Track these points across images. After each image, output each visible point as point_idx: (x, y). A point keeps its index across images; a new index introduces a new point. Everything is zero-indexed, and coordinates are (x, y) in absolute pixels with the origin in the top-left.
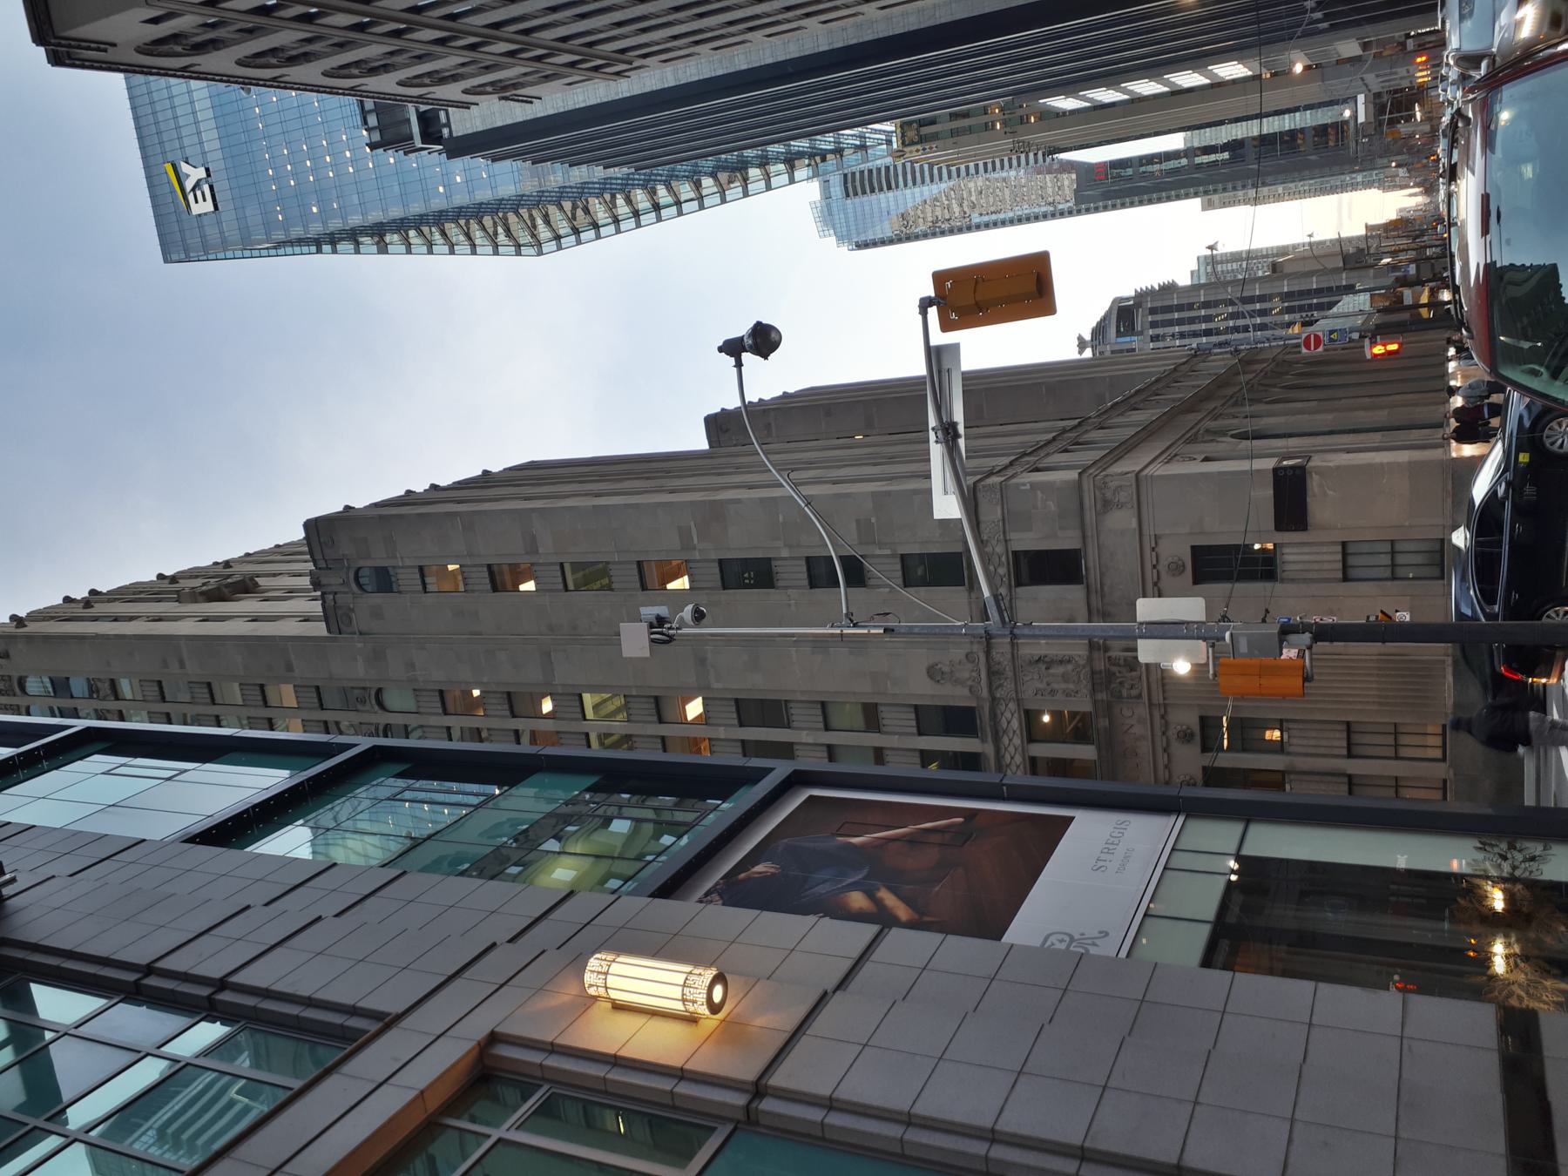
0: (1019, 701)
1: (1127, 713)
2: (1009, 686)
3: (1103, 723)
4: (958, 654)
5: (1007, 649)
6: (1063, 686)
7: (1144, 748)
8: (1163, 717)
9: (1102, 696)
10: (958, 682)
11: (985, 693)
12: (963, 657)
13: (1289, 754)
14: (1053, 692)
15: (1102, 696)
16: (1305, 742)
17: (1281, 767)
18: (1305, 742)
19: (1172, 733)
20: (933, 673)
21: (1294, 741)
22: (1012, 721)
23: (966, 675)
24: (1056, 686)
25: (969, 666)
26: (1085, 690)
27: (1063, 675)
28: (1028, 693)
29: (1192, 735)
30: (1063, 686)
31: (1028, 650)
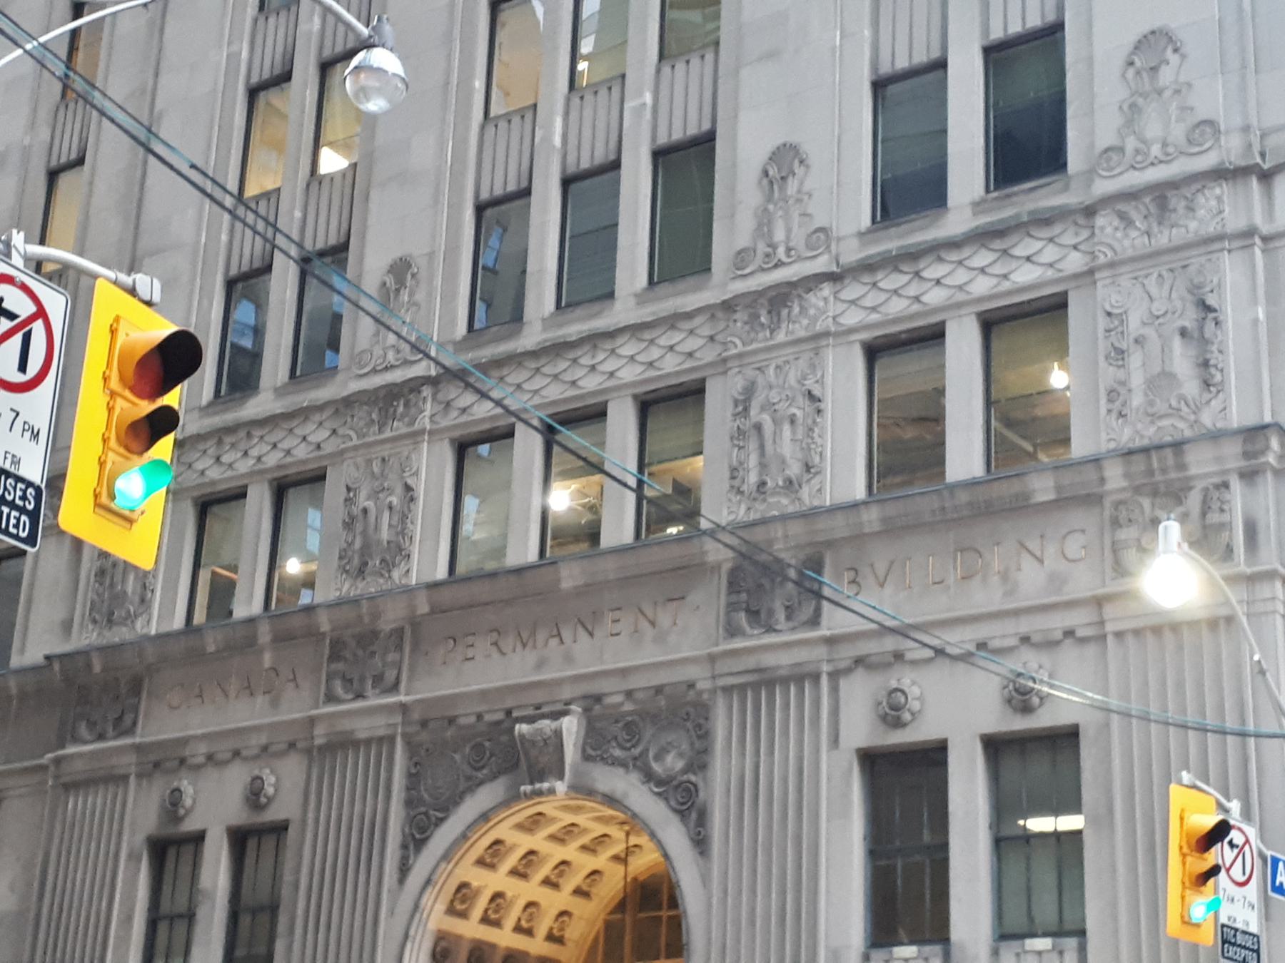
0: (1089, 274)
1: (1074, 546)
2: (1131, 242)
3: (1042, 487)
4: (1212, 99)
5: (1235, 222)
6: (1137, 380)
7: (984, 597)
8: (1069, 633)
9: (1115, 476)
10: (1132, 112)
11: (1103, 187)
12: (1202, 114)
14: (1119, 354)
15: (1115, 476)
19: (1028, 661)
20: (1154, 45)
22: (1028, 270)
23: (1153, 129)
24: (1135, 360)
25: (1178, 132)
26: (1126, 436)
27: (1167, 376)
28: (1108, 294)
30: (1137, 380)
31: (1233, 279)
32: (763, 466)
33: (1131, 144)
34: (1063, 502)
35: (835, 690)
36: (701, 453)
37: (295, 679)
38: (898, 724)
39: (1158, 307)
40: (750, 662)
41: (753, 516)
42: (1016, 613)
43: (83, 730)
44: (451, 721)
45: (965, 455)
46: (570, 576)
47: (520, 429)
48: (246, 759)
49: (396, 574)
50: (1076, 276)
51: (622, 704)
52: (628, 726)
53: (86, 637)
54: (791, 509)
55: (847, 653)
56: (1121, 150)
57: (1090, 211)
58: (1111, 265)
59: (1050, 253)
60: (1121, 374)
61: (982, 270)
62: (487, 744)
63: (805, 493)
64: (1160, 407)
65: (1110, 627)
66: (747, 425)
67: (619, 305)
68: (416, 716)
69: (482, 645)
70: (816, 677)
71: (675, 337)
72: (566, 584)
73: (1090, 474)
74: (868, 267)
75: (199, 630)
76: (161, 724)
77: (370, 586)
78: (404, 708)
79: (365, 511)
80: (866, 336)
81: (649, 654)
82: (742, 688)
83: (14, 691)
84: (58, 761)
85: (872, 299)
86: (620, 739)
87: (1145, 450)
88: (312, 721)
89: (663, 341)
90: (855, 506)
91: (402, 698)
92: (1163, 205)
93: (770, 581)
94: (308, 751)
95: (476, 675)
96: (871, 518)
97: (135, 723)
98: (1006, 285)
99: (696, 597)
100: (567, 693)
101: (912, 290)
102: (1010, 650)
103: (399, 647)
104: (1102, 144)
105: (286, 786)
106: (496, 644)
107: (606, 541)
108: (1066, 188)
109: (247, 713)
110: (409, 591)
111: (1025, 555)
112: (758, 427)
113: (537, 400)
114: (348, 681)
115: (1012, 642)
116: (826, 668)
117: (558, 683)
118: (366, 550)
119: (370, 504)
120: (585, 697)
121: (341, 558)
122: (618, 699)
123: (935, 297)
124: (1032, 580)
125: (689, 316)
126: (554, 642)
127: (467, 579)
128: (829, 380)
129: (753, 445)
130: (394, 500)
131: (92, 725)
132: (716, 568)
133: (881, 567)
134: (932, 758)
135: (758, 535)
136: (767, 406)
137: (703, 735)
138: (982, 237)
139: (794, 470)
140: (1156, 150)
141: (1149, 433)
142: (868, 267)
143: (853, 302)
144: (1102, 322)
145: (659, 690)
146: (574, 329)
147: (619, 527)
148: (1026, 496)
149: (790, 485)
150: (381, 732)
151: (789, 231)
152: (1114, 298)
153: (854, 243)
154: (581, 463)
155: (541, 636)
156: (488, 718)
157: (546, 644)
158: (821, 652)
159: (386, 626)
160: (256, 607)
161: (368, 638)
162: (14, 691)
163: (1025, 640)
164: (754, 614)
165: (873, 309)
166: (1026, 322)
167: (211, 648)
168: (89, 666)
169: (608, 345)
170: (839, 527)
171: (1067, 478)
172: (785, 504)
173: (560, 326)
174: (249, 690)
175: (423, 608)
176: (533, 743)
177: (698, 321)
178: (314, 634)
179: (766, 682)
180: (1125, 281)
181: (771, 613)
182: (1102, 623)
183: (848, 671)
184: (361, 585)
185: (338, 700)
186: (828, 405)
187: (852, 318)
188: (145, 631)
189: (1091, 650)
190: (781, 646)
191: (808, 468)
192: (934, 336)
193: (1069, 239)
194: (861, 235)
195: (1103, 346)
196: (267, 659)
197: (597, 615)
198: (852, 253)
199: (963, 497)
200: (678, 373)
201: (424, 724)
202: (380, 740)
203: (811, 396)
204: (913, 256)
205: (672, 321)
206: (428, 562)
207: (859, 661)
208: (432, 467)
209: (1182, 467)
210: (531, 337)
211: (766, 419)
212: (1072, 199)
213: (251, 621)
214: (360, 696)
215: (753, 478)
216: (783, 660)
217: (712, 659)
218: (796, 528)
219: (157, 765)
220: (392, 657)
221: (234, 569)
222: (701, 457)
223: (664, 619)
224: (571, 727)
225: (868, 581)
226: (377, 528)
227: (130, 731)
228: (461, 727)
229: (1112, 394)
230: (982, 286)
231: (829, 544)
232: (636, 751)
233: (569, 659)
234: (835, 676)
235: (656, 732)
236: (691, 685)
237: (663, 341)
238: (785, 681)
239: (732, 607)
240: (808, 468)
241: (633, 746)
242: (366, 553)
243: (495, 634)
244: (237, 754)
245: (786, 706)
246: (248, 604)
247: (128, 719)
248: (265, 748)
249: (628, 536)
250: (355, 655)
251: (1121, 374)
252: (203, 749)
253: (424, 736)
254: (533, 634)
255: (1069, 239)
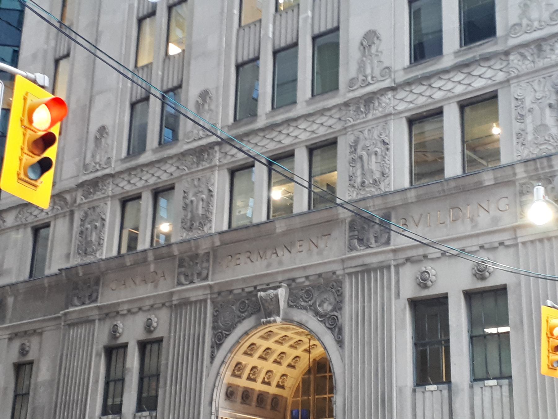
1: (503, 204)
2: (526, 66)
3: (488, 178)
6: (530, 128)
8: (501, 244)
11: (512, 42)
13: (471, 387)
14: (521, 118)
16: (487, 404)
17: (454, 379)
18: (487, 404)
19: (484, 256)
21: (487, 393)
22: (479, 81)
23: (534, 15)
24: (529, 119)
25: (546, 15)
26: (526, 154)
27: (544, 126)
28: (516, 90)
29: (483, 278)
30: (530, 128)
32: (363, 174)
33: (525, 22)
34: (498, 184)
35: (397, 273)
36: (336, 170)
37: (164, 276)
38: (426, 287)
39: (539, 95)
40: (359, 262)
41: (360, 197)
42: (478, 235)
43: (76, 301)
44: (231, 292)
45: (453, 165)
46: (280, 227)
47: (257, 163)
48: (144, 311)
49: (205, 229)
50: (501, 83)
51: (304, 282)
52: (307, 292)
53: (75, 261)
54: (376, 193)
55: (402, 256)
56: (520, 25)
57: (507, 53)
58: (517, 77)
59: (490, 73)
60: (522, 126)
61: (459, 82)
62: (247, 302)
63: (382, 186)
64: (541, 140)
65: (520, 240)
66: (355, 156)
67: (299, 106)
68: (216, 290)
69: (243, 258)
70: (389, 267)
71: (323, 119)
72: (278, 230)
73: (509, 171)
74: (408, 83)
75: (123, 256)
76: (109, 297)
77: (195, 234)
78: (210, 287)
79: (192, 202)
80: (408, 114)
81: (316, 260)
82: (356, 273)
83: (46, 285)
84: (65, 314)
85: (410, 98)
86: (304, 298)
87: (534, 160)
88: (172, 294)
89: (318, 121)
90: (404, 190)
91: (210, 283)
92: (539, 48)
93: (367, 225)
94: (171, 307)
95: (240, 272)
96: (412, 194)
97: (97, 298)
98: (470, 88)
99: (336, 233)
100: (280, 278)
101: (428, 93)
102: (475, 252)
103: (208, 261)
104: (511, 23)
105: (162, 322)
106: (249, 258)
107: (296, 210)
108: (496, 43)
109: (144, 291)
110: (211, 235)
111: (481, 209)
112: (361, 157)
113: (264, 150)
114: (186, 276)
115: (477, 248)
116: (393, 263)
117: (277, 273)
118: (192, 220)
119: (194, 199)
120: (289, 280)
121: (182, 222)
122: (303, 280)
123: (438, 95)
124: (484, 220)
125: (329, 109)
126: (274, 256)
127: (235, 230)
128: (392, 135)
129: (359, 165)
130: (204, 196)
131: (79, 298)
132: (344, 221)
133: (416, 218)
134: (442, 301)
135: (361, 205)
136: (365, 148)
137: (340, 295)
138: (458, 67)
139: (377, 176)
140: (536, 24)
141: (536, 152)
142: (408, 83)
143: (402, 100)
144: (514, 103)
145: (320, 275)
146: (279, 118)
147: (301, 204)
148: (481, 183)
149: (375, 182)
150: (201, 298)
151: (372, 69)
152: (519, 91)
153: (402, 73)
154: (284, 178)
155: (269, 253)
156: (247, 290)
157: (271, 258)
158: (391, 256)
159: (201, 252)
160: (147, 245)
161: (194, 257)
162: (46, 285)
163: (482, 247)
164: (360, 240)
165: (411, 102)
166: (479, 105)
167: (128, 264)
168: (77, 274)
169: (294, 124)
170: (397, 200)
171: (499, 174)
172: (374, 191)
173: (273, 117)
174: (145, 281)
175: (218, 243)
176: (266, 300)
177: (333, 111)
178: (171, 256)
179: (367, 270)
180: (523, 84)
181: (368, 240)
182: (516, 238)
183: (403, 264)
184: (191, 234)
185: (182, 284)
186: (391, 146)
187: (401, 107)
188: (100, 257)
189: (512, 250)
190: (373, 254)
191: (383, 174)
192: (438, 113)
193: (498, 66)
194: (404, 69)
195: (514, 114)
196: (152, 267)
197: (292, 244)
198: (401, 77)
199: (452, 184)
200: (325, 135)
201: (219, 293)
202: (201, 301)
203: (384, 143)
204: (428, 77)
205: (322, 112)
206: (219, 223)
207: (408, 260)
208: (220, 181)
209: (551, 166)
210: (261, 122)
211: (364, 153)
212: (499, 48)
213: (145, 251)
214: (192, 282)
215: (359, 180)
216: (374, 260)
217: (343, 261)
218: (378, 201)
219: (107, 315)
220: (205, 265)
221: (137, 229)
222: (336, 173)
223: (321, 244)
224: (282, 293)
225: (411, 224)
226: (197, 209)
227: (95, 301)
228: (235, 294)
229: (519, 135)
230: (459, 89)
231: (394, 208)
232: (311, 303)
233: (280, 263)
234: (397, 266)
235: (320, 294)
236: (334, 273)
237: (318, 121)
238: (375, 270)
239: (351, 238)
240: (383, 174)
241: (310, 301)
242: (192, 221)
243: (249, 253)
244: (140, 309)
245: (376, 280)
246: (143, 244)
247: (94, 295)
248: (152, 306)
249: (305, 208)
250: (189, 264)
251: (522, 126)
252: (126, 307)
253: (220, 299)
254: (265, 252)
255: (498, 66)
